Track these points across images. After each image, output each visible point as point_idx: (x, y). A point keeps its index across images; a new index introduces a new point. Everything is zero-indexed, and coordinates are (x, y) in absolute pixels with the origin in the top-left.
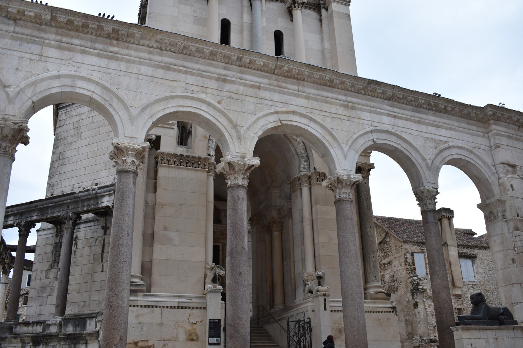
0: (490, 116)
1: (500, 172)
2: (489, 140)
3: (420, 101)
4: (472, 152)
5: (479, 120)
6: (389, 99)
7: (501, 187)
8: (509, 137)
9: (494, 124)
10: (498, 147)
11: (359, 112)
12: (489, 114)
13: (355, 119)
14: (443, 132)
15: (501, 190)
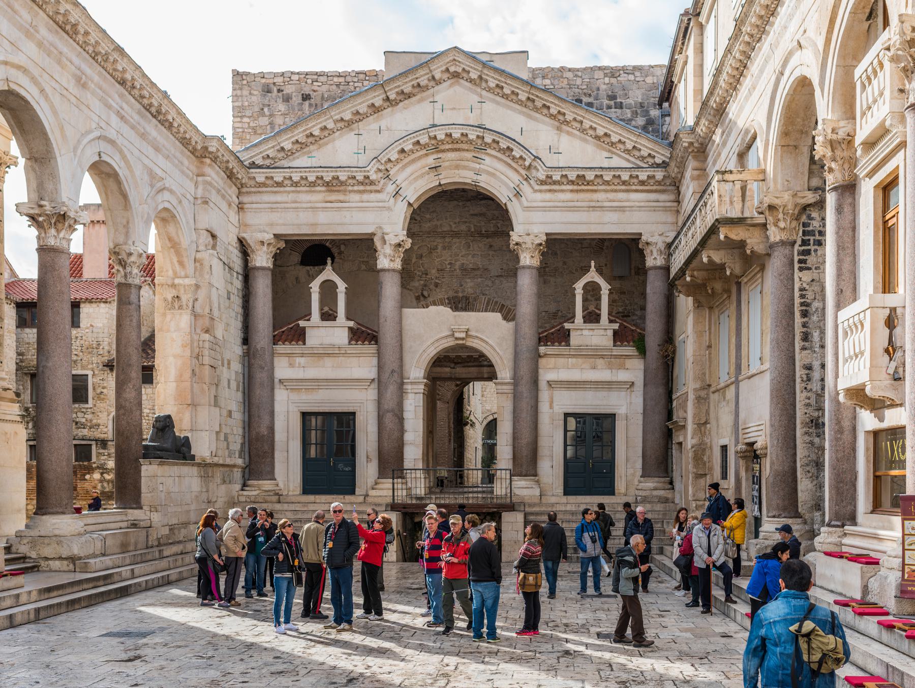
0: (211, 153)
1: (201, 241)
2: (196, 188)
3: (153, 101)
4: (180, 202)
5: (193, 152)
6: (122, 82)
7: (198, 264)
8: (218, 191)
9: (209, 165)
10: (206, 203)
11: (89, 96)
12: (210, 149)
13: (83, 107)
14: (161, 161)
15: (196, 268)
